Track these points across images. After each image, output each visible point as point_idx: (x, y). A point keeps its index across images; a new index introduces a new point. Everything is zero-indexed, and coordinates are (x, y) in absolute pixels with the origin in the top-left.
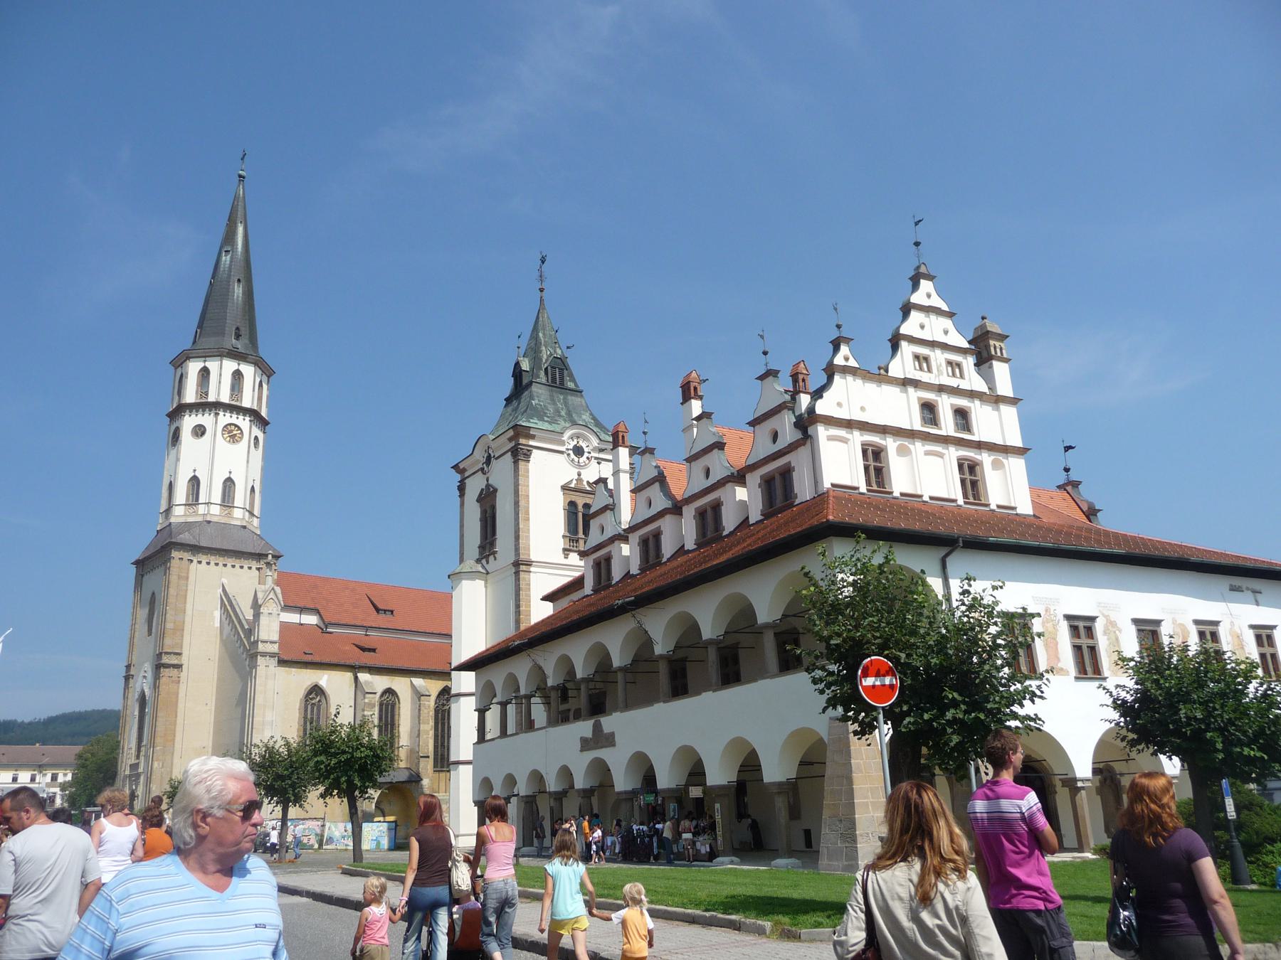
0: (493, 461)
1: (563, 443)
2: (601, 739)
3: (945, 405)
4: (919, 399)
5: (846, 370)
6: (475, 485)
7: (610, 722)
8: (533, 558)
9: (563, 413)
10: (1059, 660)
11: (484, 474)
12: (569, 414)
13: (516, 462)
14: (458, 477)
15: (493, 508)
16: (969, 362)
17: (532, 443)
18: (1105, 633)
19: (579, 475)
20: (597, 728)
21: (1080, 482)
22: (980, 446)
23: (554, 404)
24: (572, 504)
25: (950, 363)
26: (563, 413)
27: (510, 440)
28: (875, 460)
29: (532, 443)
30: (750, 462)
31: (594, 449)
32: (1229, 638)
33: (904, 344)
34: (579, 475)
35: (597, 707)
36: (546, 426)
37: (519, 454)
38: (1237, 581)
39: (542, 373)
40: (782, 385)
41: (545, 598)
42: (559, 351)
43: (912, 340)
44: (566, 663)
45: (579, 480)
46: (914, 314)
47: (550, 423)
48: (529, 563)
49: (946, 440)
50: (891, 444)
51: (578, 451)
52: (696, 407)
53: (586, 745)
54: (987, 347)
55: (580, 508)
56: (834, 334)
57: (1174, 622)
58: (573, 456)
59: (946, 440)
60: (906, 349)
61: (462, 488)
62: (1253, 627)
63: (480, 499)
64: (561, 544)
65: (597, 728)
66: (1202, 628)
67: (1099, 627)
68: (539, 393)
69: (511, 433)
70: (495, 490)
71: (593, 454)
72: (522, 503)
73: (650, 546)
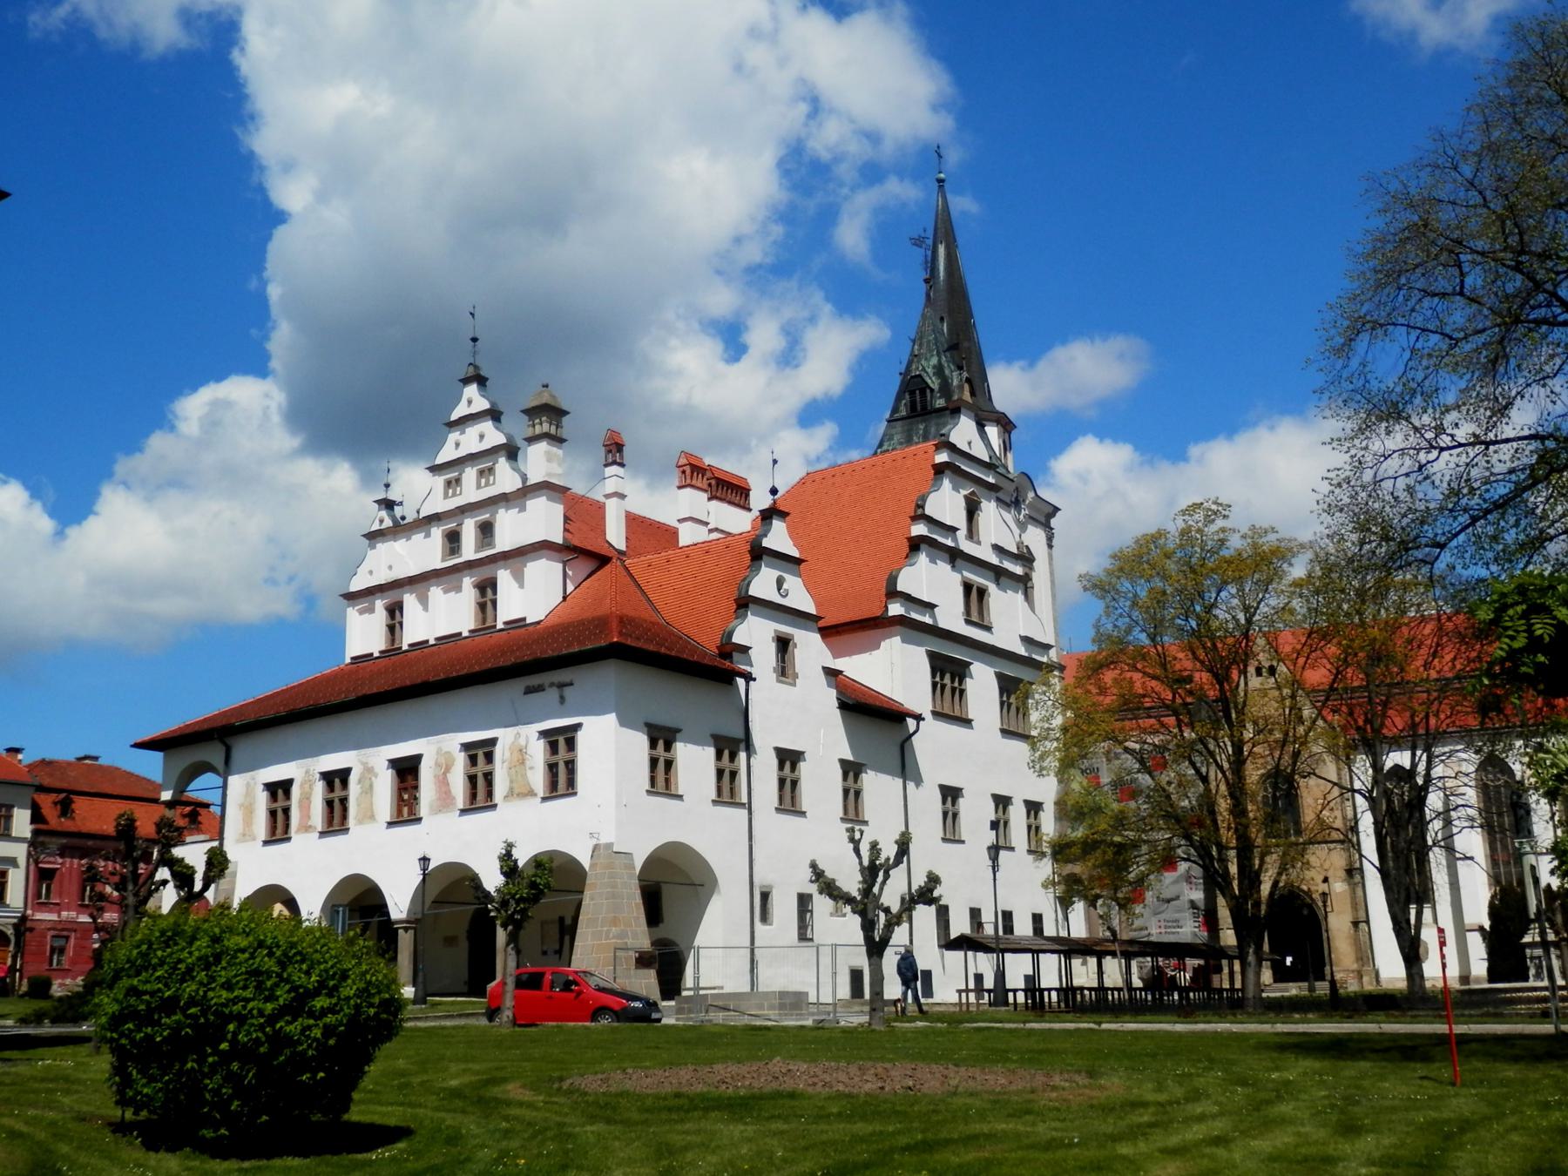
3: (469, 530)
16: (502, 464)
18: (360, 781)
32: (507, 754)
38: (534, 680)
57: (439, 751)
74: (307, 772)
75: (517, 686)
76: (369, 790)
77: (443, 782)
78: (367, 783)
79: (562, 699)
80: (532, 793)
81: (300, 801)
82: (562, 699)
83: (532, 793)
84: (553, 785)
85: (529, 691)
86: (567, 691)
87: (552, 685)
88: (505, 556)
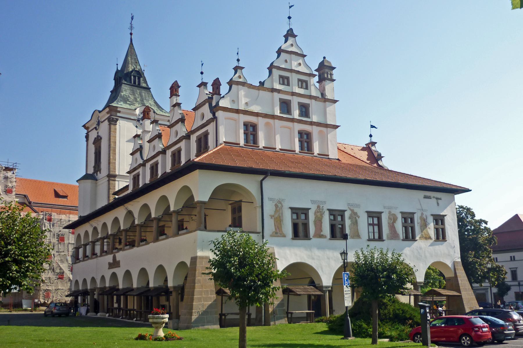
0: (101, 124)
4: (280, 99)
5: (238, 83)
6: (93, 135)
8: (117, 173)
9: (138, 100)
10: (322, 231)
11: (96, 130)
12: (142, 100)
13: (110, 124)
14: (86, 131)
15: (100, 147)
17: (118, 114)
18: (350, 218)
21: (376, 143)
22: (312, 123)
23: (134, 94)
25: (299, 80)
27: (108, 113)
28: (251, 131)
32: (419, 221)
33: (274, 71)
35: (113, 249)
36: (127, 106)
37: (112, 121)
40: (210, 89)
42: (138, 67)
43: (279, 68)
46: (283, 54)
47: (130, 105)
48: (115, 176)
49: (293, 120)
50: (261, 122)
52: (175, 100)
54: (323, 74)
56: (236, 64)
57: (390, 212)
59: (293, 120)
60: (276, 73)
61: (87, 137)
62: (432, 215)
63: (94, 143)
66: (405, 216)
67: (347, 215)
68: (126, 90)
70: (101, 138)
72: (112, 145)
73: (154, 169)
74: (318, 207)
75: (421, 194)
76: (355, 223)
77: (392, 227)
78: (354, 220)
79: (438, 204)
80: (430, 238)
81: (315, 222)
82: (438, 204)
83: (430, 238)
84: (438, 238)
85: (426, 197)
86: (439, 201)
87: (434, 197)
88: (318, 124)
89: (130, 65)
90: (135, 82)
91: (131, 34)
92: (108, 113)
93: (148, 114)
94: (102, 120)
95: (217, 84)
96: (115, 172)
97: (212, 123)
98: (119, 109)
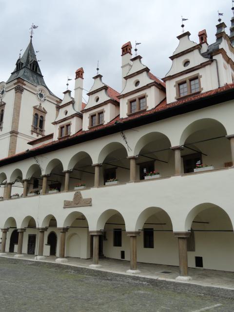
1: (36, 90)
2: (78, 201)
7: (86, 193)
8: (19, 131)
9: (36, 81)
19: (40, 104)
20: (78, 197)
23: (33, 77)
24: (36, 114)
26: (36, 81)
27: (15, 84)
29: (24, 87)
30: (171, 74)
31: (48, 97)
34: (40, 104)
37: (19, 90)
39: (29, 65)
41: (29, 143)
44: (57, 165)
45: (40, 106)
48: (17, 133)
51: (41, 95)
53: (67, 205)
55: (39, 117)
56: (218, 23)
58: (39, 97)
64: (30, 128)
65: (78, 197)
69: (16, 81)
70: (5, 104)
71: (47, 98)
89: (30, 57)
90: (33, 69)
91: (31, 37)
92: (15, 84)
93: (82, 74)
94: (7, 90)
95: (203, 36)
96: (18, 130)
97: (208, 67)
98: (25, 82)
